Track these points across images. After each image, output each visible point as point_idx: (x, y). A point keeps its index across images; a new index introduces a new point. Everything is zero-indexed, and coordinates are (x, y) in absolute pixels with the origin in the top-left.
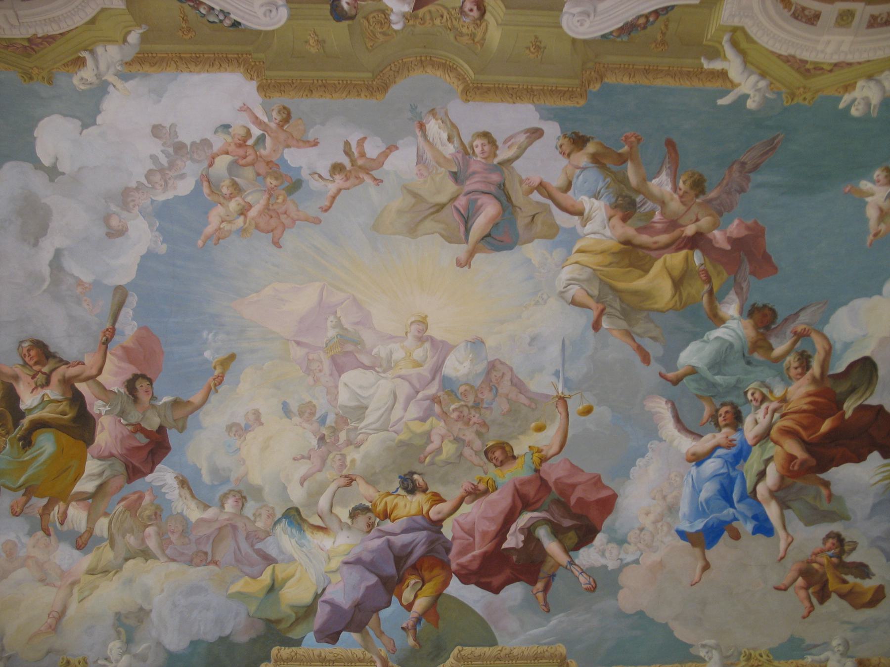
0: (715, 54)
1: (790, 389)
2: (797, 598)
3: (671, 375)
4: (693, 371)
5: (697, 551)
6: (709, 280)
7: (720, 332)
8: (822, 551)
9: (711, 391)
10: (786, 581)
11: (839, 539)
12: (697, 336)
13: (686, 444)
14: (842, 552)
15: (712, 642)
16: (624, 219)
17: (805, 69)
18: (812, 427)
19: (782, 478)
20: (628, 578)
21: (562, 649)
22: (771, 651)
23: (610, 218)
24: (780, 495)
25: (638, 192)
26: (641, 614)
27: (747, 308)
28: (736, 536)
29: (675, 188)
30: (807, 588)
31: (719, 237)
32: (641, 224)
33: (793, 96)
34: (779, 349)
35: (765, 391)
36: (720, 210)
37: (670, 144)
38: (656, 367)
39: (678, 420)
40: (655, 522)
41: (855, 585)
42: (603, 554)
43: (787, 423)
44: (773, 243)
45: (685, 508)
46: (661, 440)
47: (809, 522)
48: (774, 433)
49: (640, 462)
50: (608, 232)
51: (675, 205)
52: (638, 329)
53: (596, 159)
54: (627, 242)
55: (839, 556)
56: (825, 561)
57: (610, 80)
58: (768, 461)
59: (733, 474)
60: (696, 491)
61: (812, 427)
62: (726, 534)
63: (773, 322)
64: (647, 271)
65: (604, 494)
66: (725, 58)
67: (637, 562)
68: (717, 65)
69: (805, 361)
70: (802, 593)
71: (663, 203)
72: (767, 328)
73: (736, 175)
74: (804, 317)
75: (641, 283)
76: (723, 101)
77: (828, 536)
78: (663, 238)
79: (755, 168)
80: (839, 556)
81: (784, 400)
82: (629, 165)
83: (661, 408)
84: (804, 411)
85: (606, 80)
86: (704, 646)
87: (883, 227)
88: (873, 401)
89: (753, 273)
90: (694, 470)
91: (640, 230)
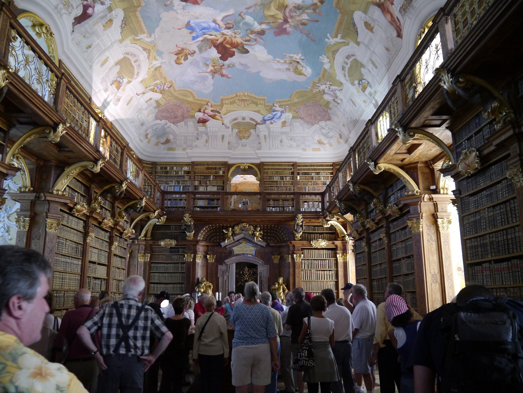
0: (342, 38)
1: (239, 39)
2: (176, 50)
3: (242, 14)
4: (243, 19)
5: (185, 26)
6: (273, 22)
7: (256, 24)
8: (190, 51)
9: (237, 23)
10: (179, 46)
11: (195, 52)
12: (255, 19)
13: (219, 19)
14: (190, 54)
15: (156, 37)
16: (294, 7)
17: (334, 52)
18: (227, 43)
19: (211, 39)
20: (171, 13)
21: (143, 4)
22: (158, 50)
23: (295, 4)
24: (205, 40)
25: (303, 11)
26: (161, 19)
27: (264, 30)
28: (190, 33)
29: (303, 19)
30: (178, 51)
31: (287, 26)
32: (292, 10)
33: (328, 48)
34: (251, 36)
35: (238, 33)
36: (295, 27)
37: (317, 21)
38: (244, 11)
39: (227, 16)
40: (192, 15)
41: (181, 59)
42: (178, 5)
43: (228, 38)
44: (284, 37)
45: (197, 21)
46: (220, 13)
47: (198, 47)
48: (224, 36)
49: (212, 9)
50: (290, 2)
51: (298, 18)
52: (257, 7)
53: (315, 4)
54: (287, 6)
55: (189, 54)
56: (187, 51)
57: (340, 15)
58: (216, 36)
59: (211, 29)
60: (204, 22)
61: (227, 43)
62: (191, 31)
63: (260, 35)
64: (277, 10)
65: (199, 1)
66: (340, 39)
67: (178, 13)
68: (339, 36)
69: (249, 41)
70: (177, 50)
71: (299, 16)
72: (258, 33)
73: (306, 32)
74: (261, 41)
75: (273, 8)
76: (328, 35)
77: (194, 51)
78: (287, 14)
79: (308, 36)
80: (189, 54)
81: (235, 37)
82: (312, 11)
83: (231, 12)
84: (232, 41)
85: (340, 14)
86: (155, 36)
87: (288, 56)
88: (236, 53)
89: (275, 32)
90: (211, 21)
91: (291, 10)
